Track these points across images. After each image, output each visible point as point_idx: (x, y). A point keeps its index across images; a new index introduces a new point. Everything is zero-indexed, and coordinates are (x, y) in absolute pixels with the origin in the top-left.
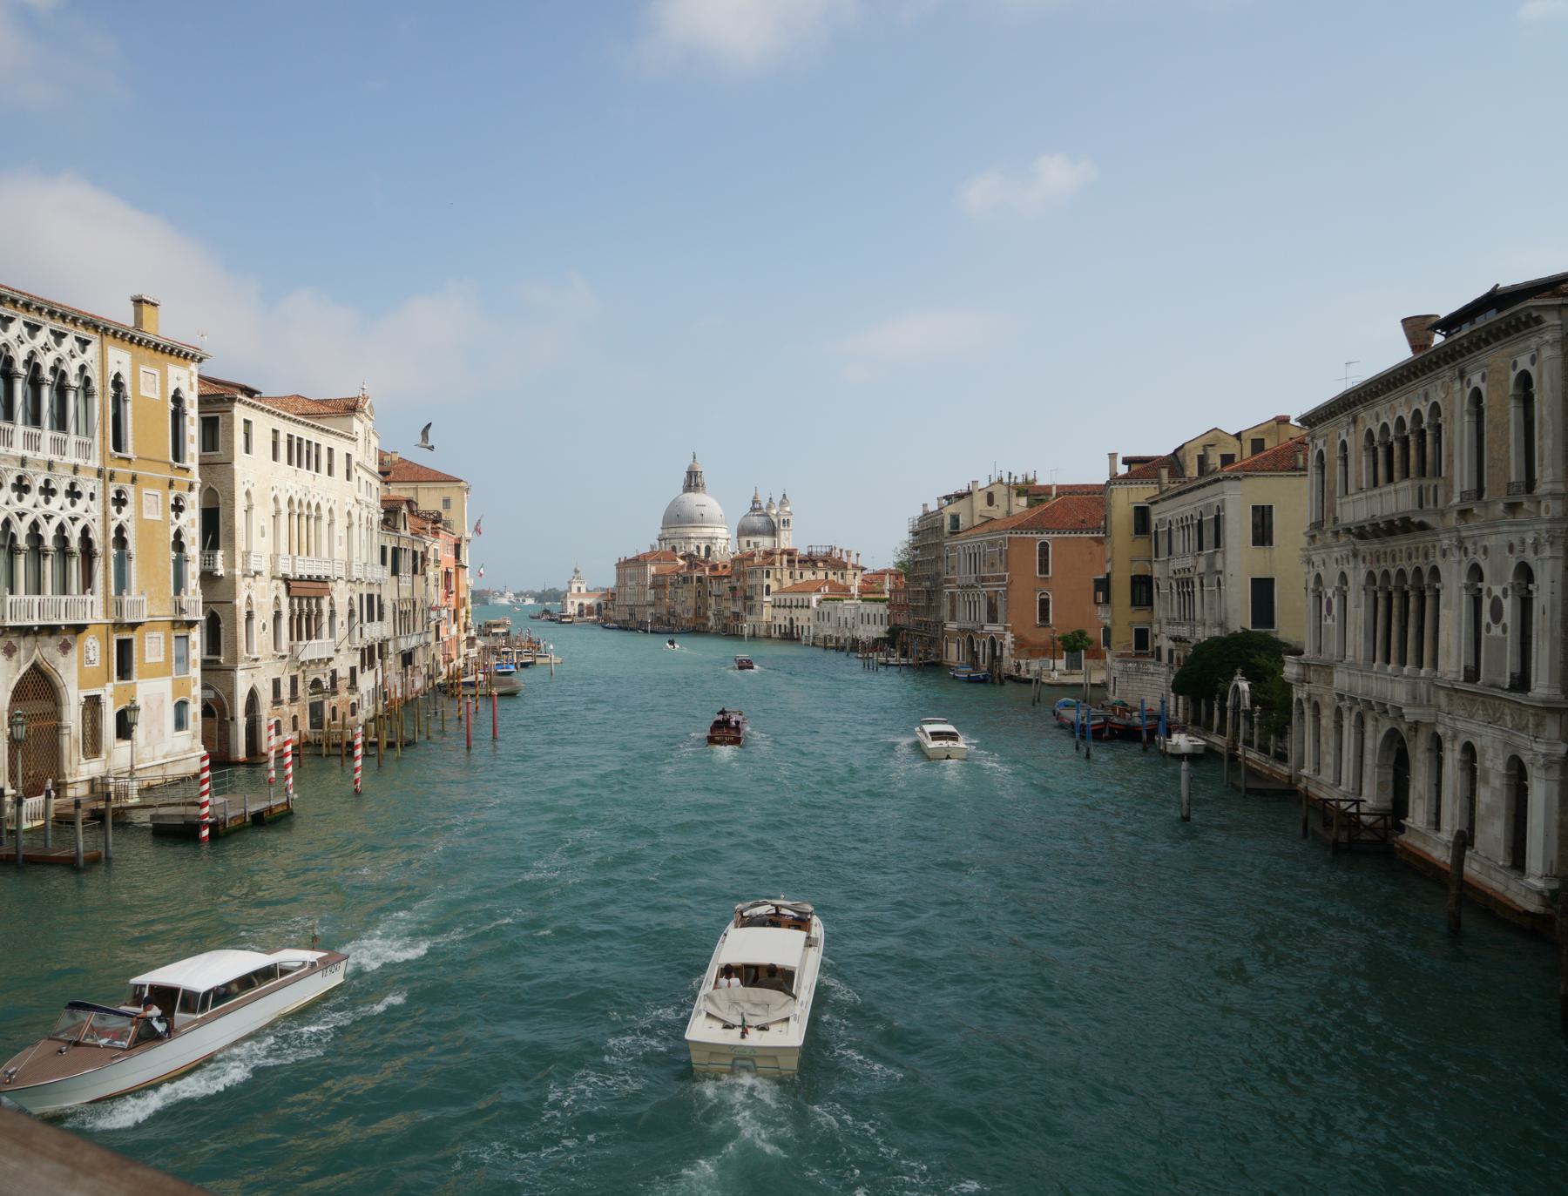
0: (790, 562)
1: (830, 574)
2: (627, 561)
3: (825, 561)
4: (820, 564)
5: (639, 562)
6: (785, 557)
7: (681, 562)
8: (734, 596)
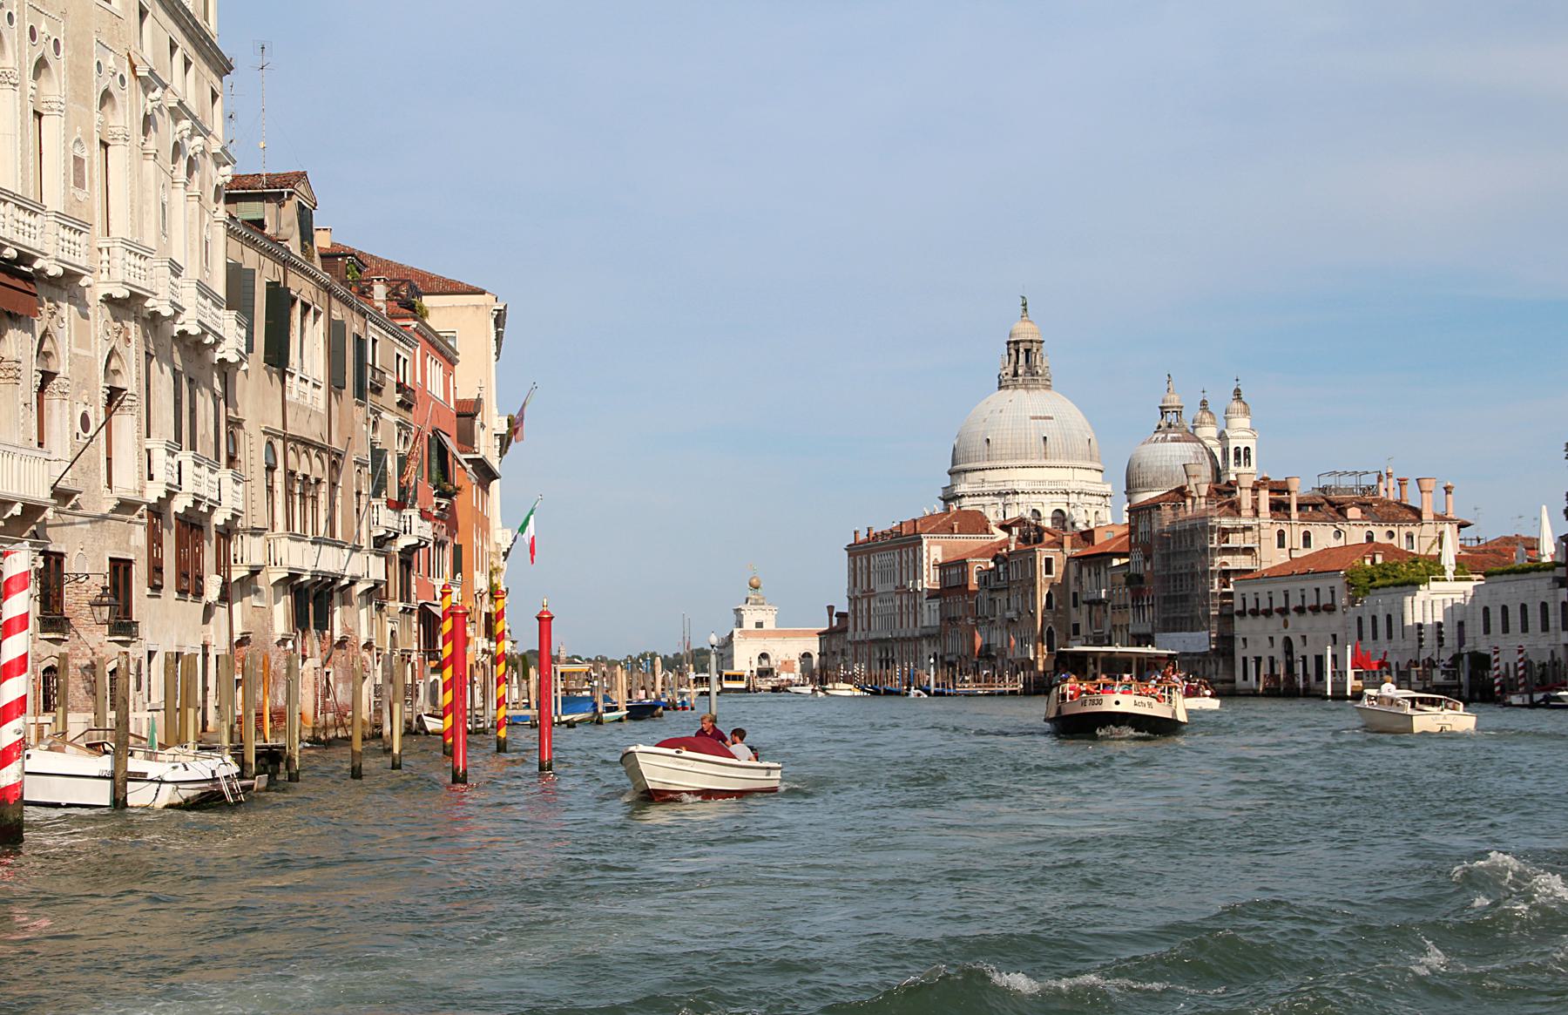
0: (1279, 508)
3: (1364, 506)
4: (1354, 513)
5: (905, 541)
6: (1265, 497)
7: (1001, 535)
8: (1137, 596)
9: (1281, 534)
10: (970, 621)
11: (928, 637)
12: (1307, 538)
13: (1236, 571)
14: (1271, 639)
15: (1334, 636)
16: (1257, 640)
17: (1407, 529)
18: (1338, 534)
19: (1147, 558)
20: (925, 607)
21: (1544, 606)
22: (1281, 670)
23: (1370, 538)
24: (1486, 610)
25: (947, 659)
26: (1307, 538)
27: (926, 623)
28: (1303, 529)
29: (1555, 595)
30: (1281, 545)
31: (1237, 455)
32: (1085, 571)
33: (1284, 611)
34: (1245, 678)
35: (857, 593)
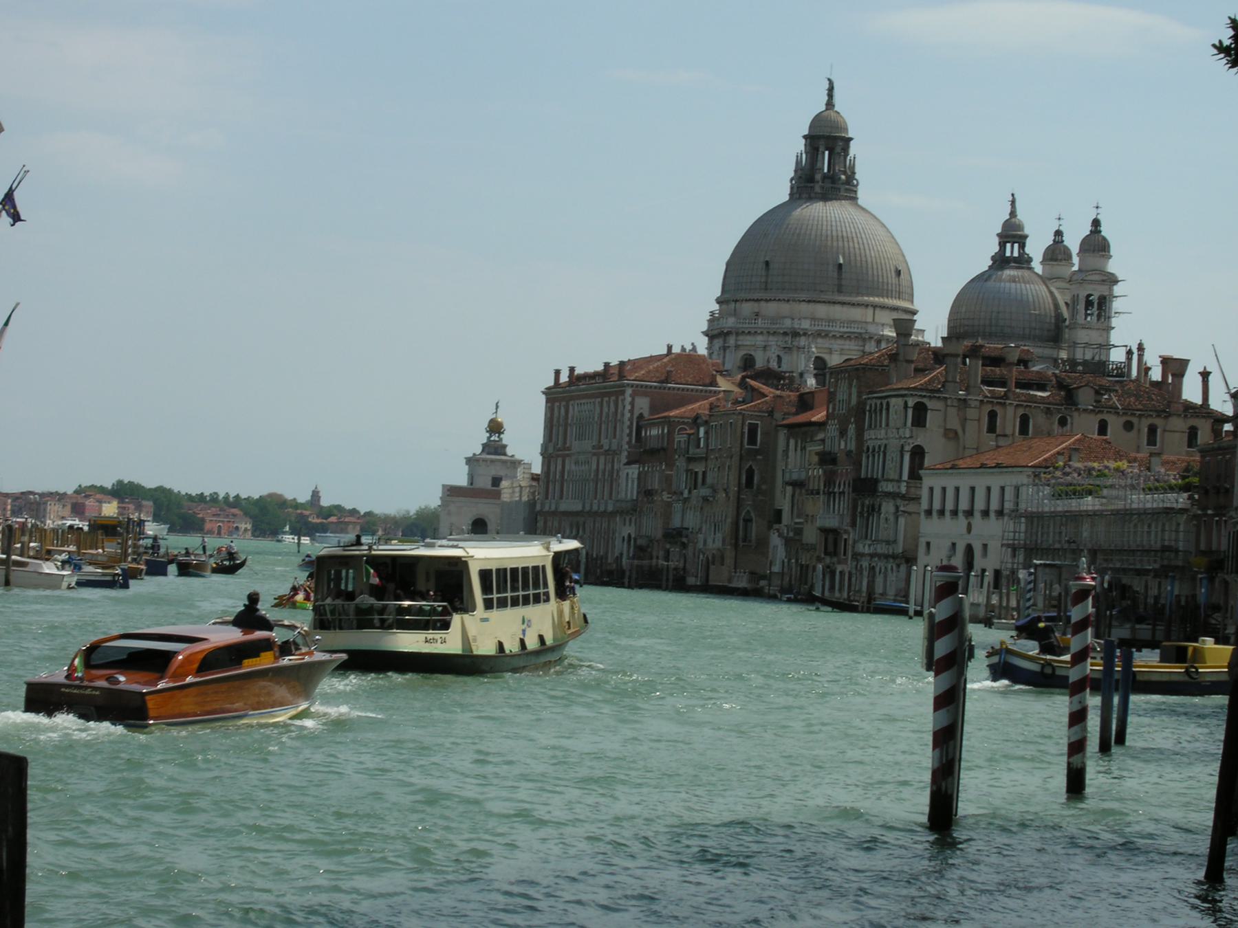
1: (1115, 423)
2: (575, 379)
6: (978, 369)
8: (830, 480)
9: (992, 416)
10: (665, 496)
11: (621, 512)
12: (1024, 420)
17: (1150, 421)
19: (843, 433)
20: (623, 475)
23: (1103, 428)
25: (639, 542)
27: (622, 496)
28: (1021, 411)
30: (992, 428)
31: (1089, 304)
32: (792, 442)
33: (970, 513)
35: (551, 450)
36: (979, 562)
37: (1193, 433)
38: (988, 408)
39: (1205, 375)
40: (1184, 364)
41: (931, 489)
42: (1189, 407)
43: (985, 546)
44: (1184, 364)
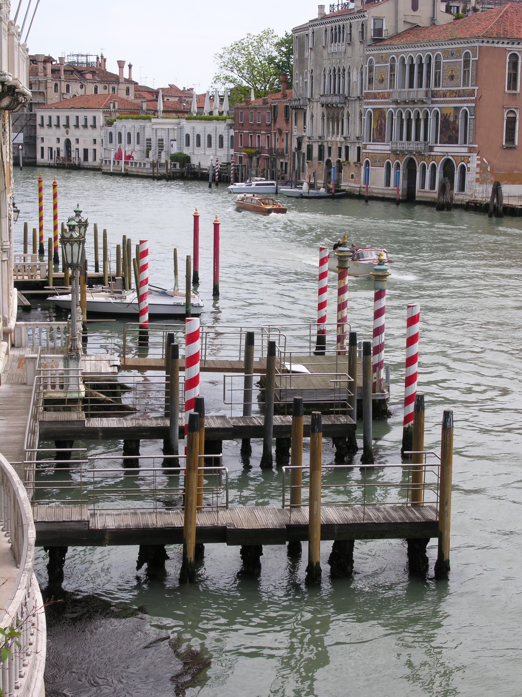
1: (100, 87)
9: (56, 85)
12: (68, 87)
13: (36, 103)
14: (58, 140)
15: (95, 141)
16: (49, 139)
17: (113, 85)
18: (82, 87)
21: (221, 138)
22: (62, 154)
23: (96, 89)
24: (188, 136)
26: (68, 87)
28: (66, 83)
29: (228, 132)
30: (56, 91)
34: (42, 156)
36: (74, 146)
37: (128, 90)
38: (54, 83)
39: (130, 66)
40: (124, 62)
41: (42, 118)
42: (126, 80)
43: (77, 140)
44: (124, 62)
